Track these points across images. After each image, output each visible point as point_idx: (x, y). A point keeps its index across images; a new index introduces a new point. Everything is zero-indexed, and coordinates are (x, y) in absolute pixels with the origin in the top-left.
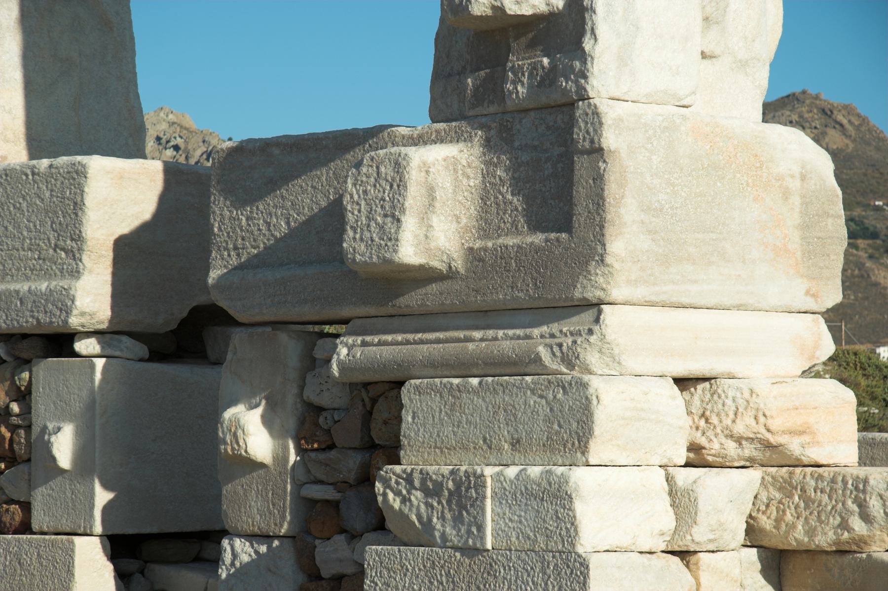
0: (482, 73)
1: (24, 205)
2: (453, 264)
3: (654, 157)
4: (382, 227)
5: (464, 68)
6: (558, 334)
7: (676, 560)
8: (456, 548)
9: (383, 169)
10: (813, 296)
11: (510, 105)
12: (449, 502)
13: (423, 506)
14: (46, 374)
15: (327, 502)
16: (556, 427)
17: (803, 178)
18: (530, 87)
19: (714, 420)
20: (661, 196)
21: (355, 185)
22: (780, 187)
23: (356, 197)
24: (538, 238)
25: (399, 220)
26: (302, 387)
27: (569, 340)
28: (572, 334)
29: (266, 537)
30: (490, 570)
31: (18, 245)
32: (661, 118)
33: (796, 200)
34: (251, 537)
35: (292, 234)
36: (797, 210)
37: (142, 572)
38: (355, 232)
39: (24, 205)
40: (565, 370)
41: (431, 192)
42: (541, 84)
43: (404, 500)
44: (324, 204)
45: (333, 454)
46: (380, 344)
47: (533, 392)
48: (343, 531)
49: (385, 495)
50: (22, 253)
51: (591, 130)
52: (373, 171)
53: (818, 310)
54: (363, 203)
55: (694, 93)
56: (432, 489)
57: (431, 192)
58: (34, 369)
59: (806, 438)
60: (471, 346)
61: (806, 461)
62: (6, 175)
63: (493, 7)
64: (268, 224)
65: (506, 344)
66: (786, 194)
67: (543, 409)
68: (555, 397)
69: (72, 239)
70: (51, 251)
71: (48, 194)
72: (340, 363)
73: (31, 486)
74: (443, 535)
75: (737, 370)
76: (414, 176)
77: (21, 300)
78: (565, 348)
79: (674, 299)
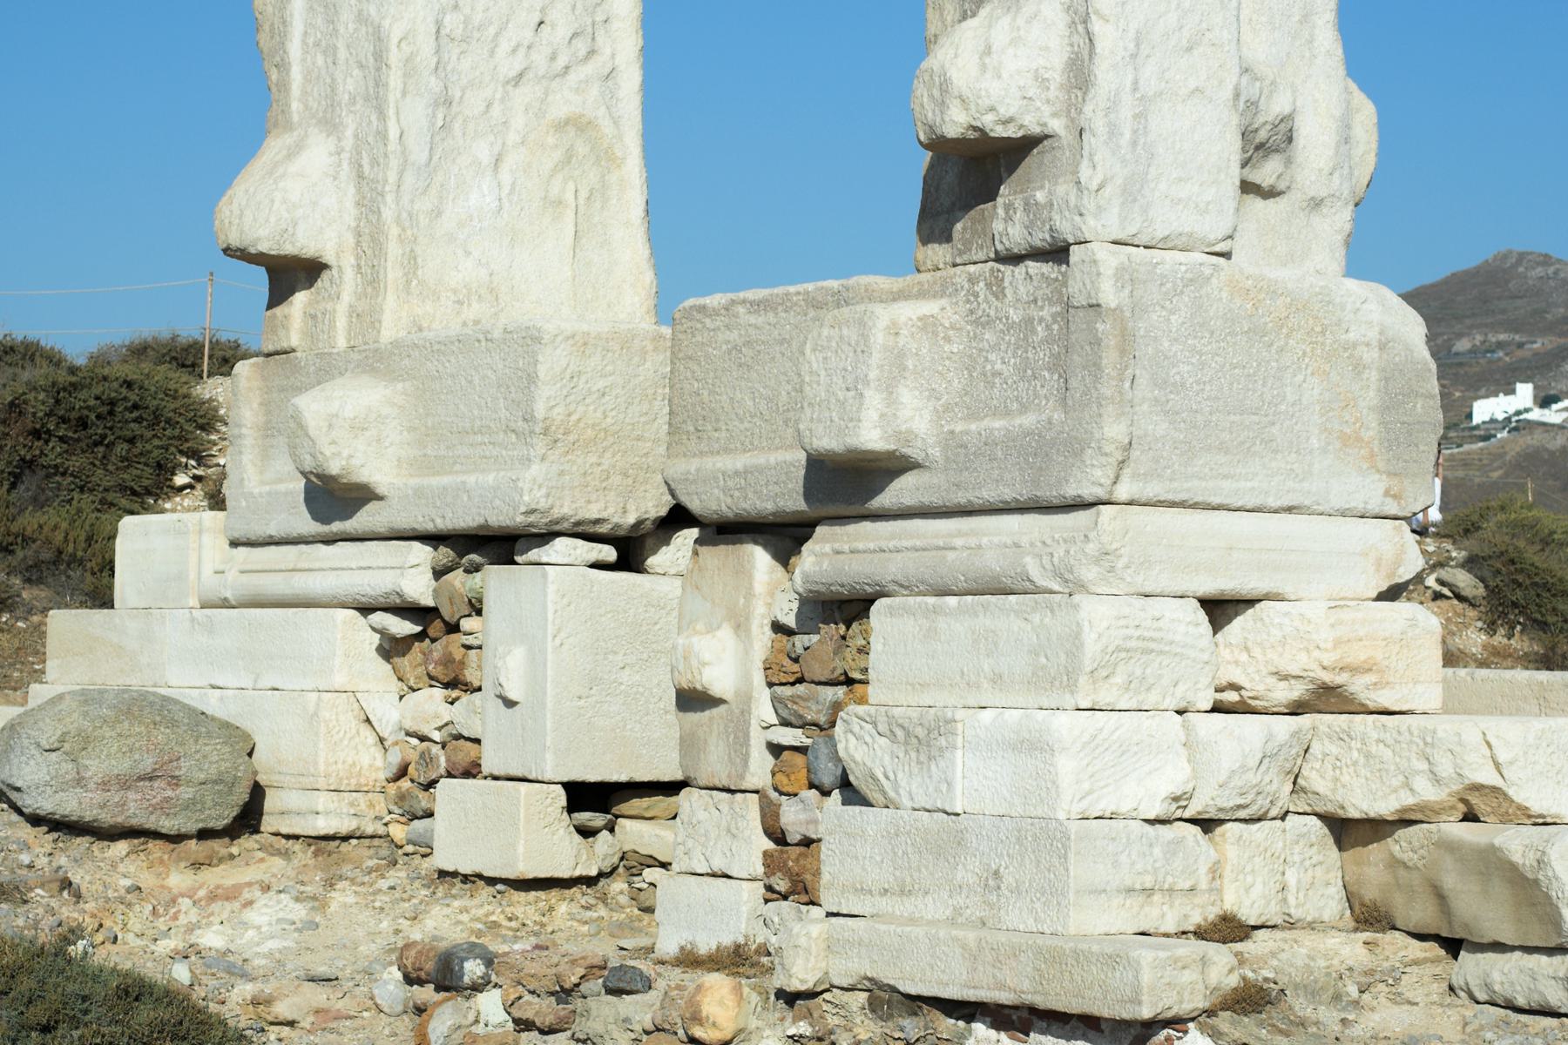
2: (930, 451)
3: (1173, 318)
4: (842, 404)
5: (953, 204)
6: (1049, 542)
7: (1196, 830)
10: (1395, 497)
13: (887, 758)
16: (1044, 660)
17: (1382, 347)
19: (1257, 652)
20: (1185, 368)
21: (814, 350)
22: (1351, 356)
23: (815, 366)
27: (1063, 547)
28: (1065, 541)
32: (1183, 268)
33: (1374, 375)
36: (1373, 387)
37: (612, 830)
40: (1056, 587)
48: (812, 786)
51: (1087, 282)
53: (1401, 514)
55: (1231, 237)
59: (1370, 678)
60: (951, 555)
61: (1371, 706)
66: (1359, 368)
72: (803, 573)
75: (1287, 589)
78: (1056, 560)
79: (1199, 499)
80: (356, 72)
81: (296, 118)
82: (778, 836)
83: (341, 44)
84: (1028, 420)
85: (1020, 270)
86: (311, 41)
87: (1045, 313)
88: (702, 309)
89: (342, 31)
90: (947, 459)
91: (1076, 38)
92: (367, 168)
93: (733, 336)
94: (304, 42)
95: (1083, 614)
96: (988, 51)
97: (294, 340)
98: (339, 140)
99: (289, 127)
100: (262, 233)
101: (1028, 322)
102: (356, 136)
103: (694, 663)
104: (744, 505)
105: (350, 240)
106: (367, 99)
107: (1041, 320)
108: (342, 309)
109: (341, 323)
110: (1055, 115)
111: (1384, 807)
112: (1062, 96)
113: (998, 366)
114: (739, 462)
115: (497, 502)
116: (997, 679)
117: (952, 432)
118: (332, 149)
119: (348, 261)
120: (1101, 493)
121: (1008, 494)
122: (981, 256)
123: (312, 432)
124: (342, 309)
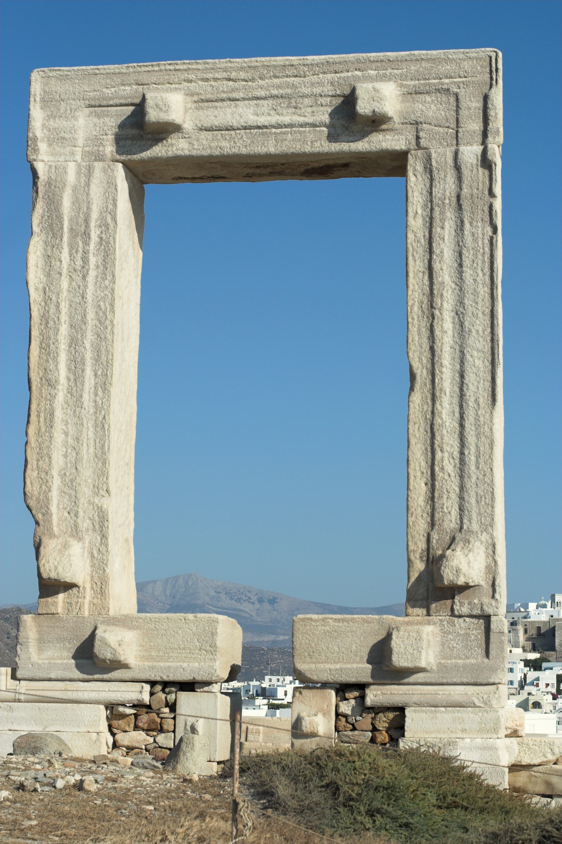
2: (433, 667)
9: (411, 634)
16: (484, 725)
23: (398, 642)
25: (420, 652)
38: (398, 655)
39: (180, 632)
40: (482, 706)
41: (429, 642)
45: (356, 732)
47: (472, 713)
50: (179, 651)
54: (402, 645)
57: (429, 642)
60: (439, 697)
63: (465, 582)
68: (483, 715)
70: (197, 651)
71: (195, 628)
76: (424, 636)
78: (484, 699)
80: (88, 521)
81: (56, 533)
84: (473, 661)
85: (461, 620)
86: (61, 507)
87: (474, 632)
88: (311, 619)
89: (81, 506)
90: (438, 670)
91: (488, 560)
92: (96, 555)
93: (327, 628)
94: (58, 507)
95: (499, 713)
96: (469, 562)
97: (60, 610)
98: (84, 543)
99: (52, 536)
100: (68, 575)
101: (467, 635)
102: (90, 543)
103: (315, 725)
104: (341, 679)
105: (88, 578)
106: (94, 530)
107: (473, 634)
108: (87, 601)
109: (86, 606)
110: (482, 580)
111: (536, 762)
112: (484, 575)
113: (455, 645)
114: (338, 666)
115: (202, 673)
116: (464, 731)
117: (440, 663)
118: (81, 546)
119: (88, 586)
120: (500, 681)
121: (465, 680)
122: (444, 614)
123: (112, 646)
124: (87, 601)
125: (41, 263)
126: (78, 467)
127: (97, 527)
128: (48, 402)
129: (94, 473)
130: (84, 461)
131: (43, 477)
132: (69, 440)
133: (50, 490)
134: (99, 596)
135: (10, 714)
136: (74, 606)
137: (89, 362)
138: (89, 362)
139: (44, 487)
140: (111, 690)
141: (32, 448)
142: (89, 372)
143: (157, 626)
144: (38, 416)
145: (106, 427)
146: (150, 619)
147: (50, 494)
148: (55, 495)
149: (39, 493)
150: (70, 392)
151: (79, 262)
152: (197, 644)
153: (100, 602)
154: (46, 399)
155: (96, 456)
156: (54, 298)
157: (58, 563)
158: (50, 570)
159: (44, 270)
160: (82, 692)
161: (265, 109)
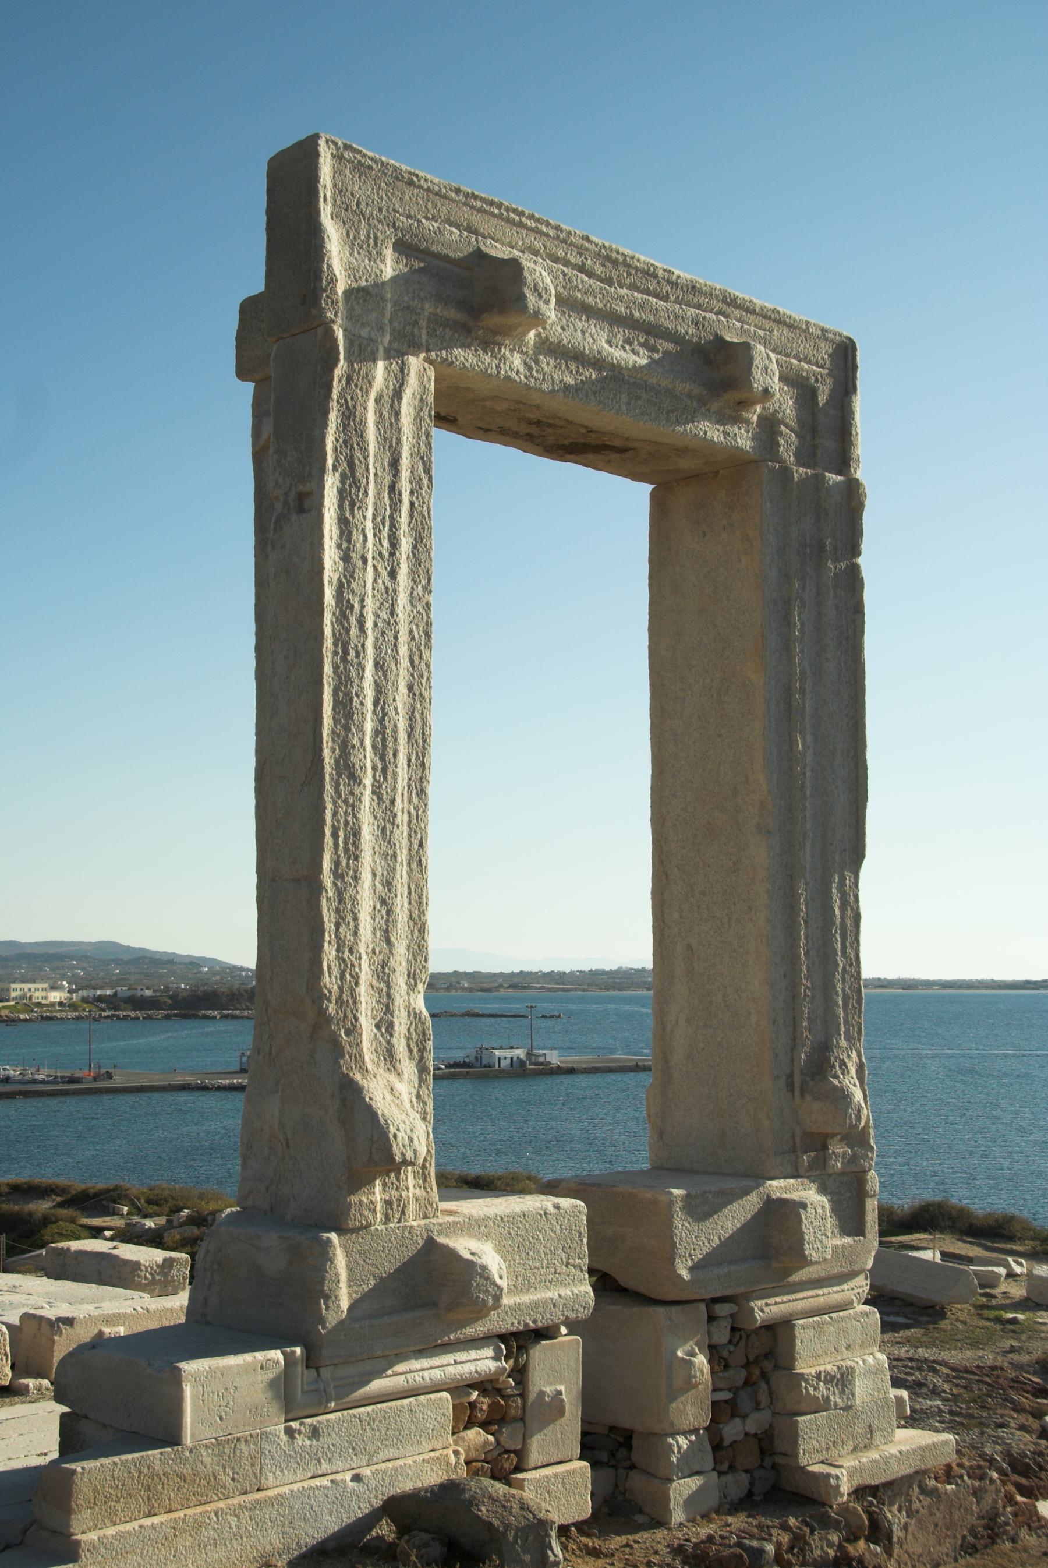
0: (812, 1154)
1: (541, 1237)
4: (821, 1242)
8: (841, 1409)
11: (831, 1171)
12: (837, 1385)
14: (540, 1354)
15: (726, 1402)
18: (842, 1163)
24: (848, 1240)
26: (709, 1333)
29: (695, 1431)
30: (856, 1417)
31: (538, 1265)
34: (685, 1433)
35: (723, 1244)
39: (541, 1237)
42: (848, 1162)
43: (815, 1389)
44: (738, 1226)
45: (731, 1372)
46: (776, 1303)
48: (733, 1416)
49: (806, 1388)
52: (813, 1211)
56: (829, 1379)
58: (531, 1352)
62: (524, 1215)
64: (709, 1240)
65: (836, 1296)
67: (859, 1328)
69: (579, 1258)
73: (525, 1439)
74: (836, 1404)
77: (554, 1305)
82: (717, 1447)
83: (395, 1020)
125: (336, 532)
126: (393, 939)
127: (415, 1050)
128: (350, 810)
129: (408, 950)
130: (399, 926)
131: (346, 957)
132: (377, 884)
133: (357, 984)
134: (421, 1182)
135: (314, 1442)
136: (395, 1206)
137: (402, 737)
138: (402, 737)
139: (348, 977)
140: (458, 1360)
141: (328, 899)
142: (402, 758)
143: (512, 1232)
144: (335, 835)
145: (423, 860)
146: (502, 1218)
147: (357, 990)
148: (363, 990)
149: (341, 988)
150: (373, 792)
151: (386, 543)
152: (564, 1255)
153: (424, 1194)
154: (346, 802)
155: (411, 916)
156: (357, 606)
157: (412, 1131)
158: (404, 1146)
159: (339, 546)
160: (420, 1373)
161: (620, 337)
